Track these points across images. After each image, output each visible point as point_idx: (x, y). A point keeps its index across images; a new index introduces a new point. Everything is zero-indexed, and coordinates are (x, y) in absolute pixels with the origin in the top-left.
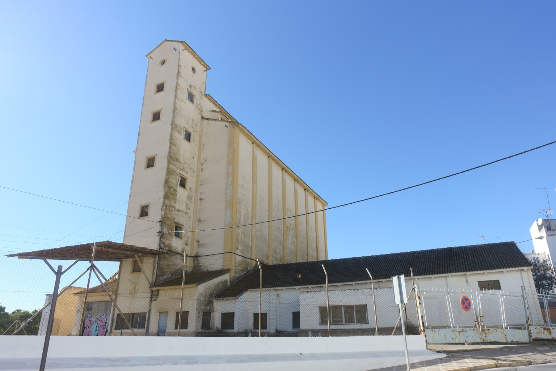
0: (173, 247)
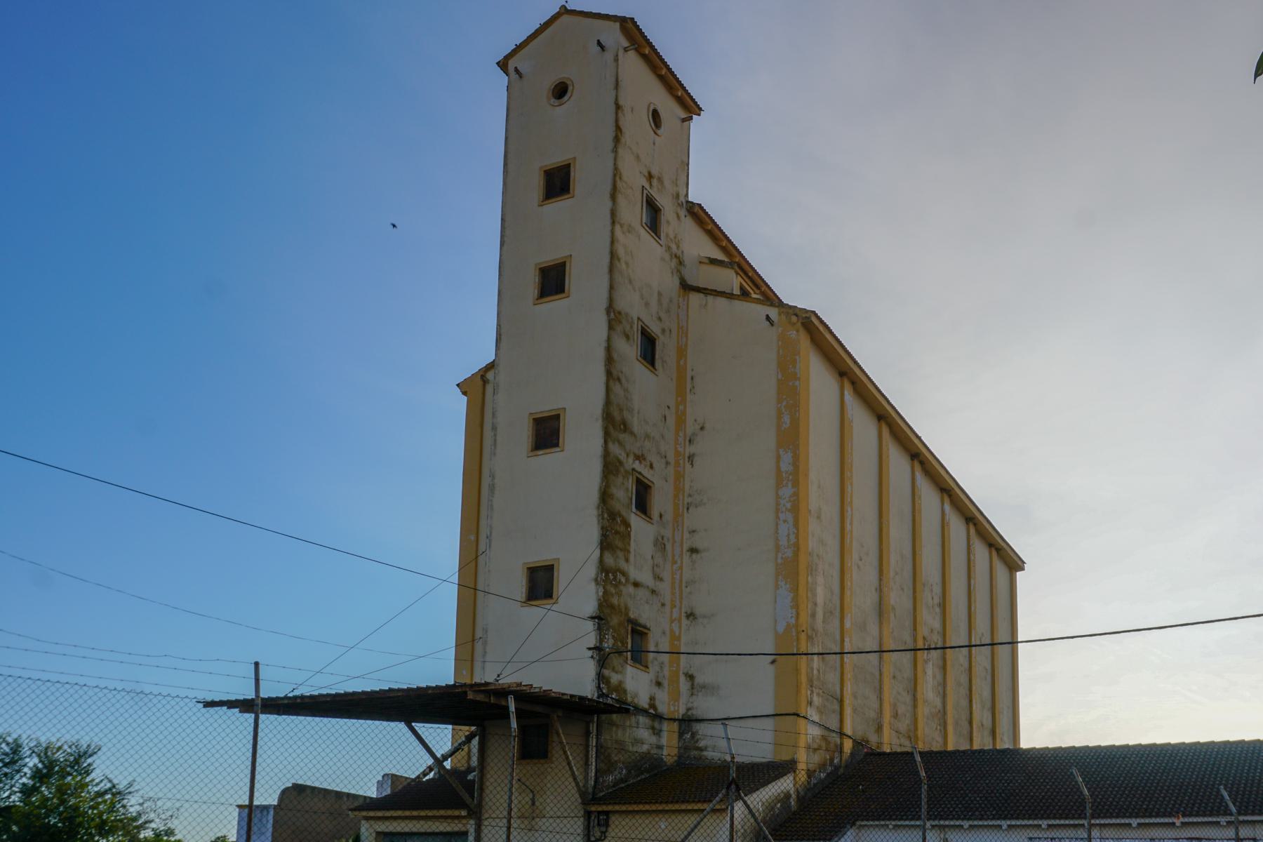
0: (628, 692)
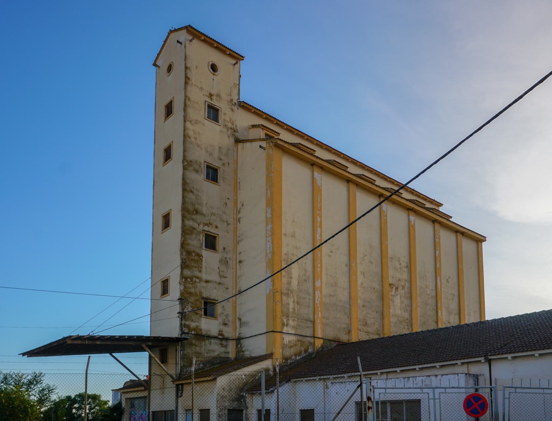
0: (203, 330)
